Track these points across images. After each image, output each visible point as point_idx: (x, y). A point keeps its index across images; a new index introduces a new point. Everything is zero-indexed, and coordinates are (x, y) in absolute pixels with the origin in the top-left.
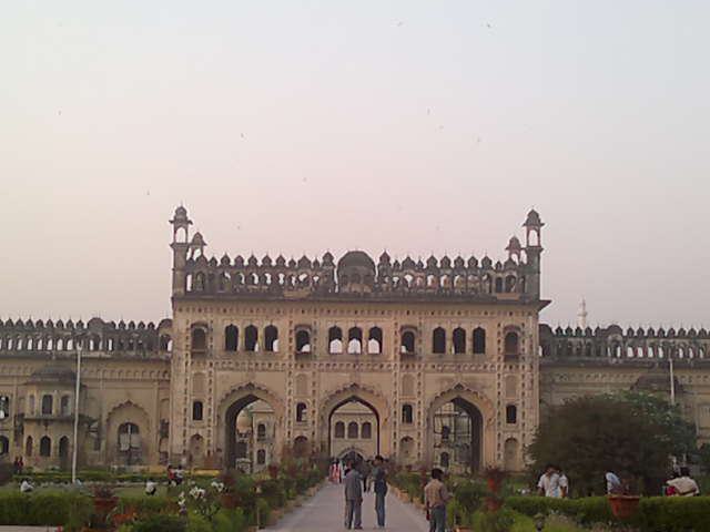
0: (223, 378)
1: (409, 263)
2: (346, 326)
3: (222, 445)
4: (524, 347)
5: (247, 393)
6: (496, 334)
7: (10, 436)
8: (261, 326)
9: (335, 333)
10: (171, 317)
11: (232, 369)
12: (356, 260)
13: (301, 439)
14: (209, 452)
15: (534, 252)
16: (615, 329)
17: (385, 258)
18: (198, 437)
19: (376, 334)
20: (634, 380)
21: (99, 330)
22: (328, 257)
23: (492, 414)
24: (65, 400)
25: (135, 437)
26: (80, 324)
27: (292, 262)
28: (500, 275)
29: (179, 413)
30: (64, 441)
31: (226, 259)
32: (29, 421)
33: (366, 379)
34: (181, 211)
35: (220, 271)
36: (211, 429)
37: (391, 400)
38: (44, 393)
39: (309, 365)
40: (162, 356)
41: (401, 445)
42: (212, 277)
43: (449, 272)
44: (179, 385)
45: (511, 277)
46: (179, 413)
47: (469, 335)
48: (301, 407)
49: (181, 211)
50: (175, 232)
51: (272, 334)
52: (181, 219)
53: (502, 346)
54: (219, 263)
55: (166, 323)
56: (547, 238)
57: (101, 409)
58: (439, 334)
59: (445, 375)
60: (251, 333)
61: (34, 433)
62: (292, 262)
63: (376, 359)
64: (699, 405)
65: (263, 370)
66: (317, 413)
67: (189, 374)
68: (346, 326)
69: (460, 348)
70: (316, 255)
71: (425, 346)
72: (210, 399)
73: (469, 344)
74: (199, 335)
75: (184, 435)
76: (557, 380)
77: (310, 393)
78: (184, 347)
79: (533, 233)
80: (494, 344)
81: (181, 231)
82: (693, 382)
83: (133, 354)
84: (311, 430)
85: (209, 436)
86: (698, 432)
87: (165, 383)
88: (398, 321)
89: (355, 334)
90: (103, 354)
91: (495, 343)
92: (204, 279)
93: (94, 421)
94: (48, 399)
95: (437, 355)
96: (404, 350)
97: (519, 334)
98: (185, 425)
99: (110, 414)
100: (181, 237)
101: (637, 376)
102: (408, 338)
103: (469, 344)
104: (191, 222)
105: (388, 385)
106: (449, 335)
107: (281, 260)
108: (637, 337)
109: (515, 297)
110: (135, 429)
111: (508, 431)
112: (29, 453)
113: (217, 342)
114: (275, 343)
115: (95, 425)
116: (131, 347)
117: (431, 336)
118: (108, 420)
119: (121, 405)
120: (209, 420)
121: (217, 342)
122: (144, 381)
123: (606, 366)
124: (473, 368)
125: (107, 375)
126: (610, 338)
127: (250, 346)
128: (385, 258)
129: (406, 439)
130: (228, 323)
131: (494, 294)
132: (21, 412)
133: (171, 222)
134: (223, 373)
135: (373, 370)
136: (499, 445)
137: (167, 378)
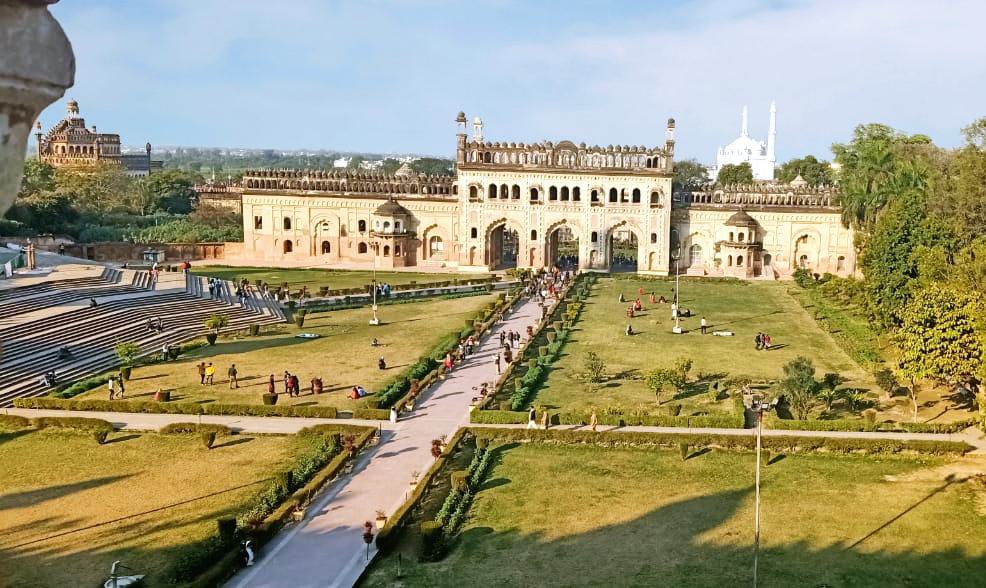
0: (489, 213)
2: (559, 181)
24: (397, 225)
33: (570, 216)
34: (463, 115)
41: (591, 255)
43: (620, 154)
44: (463, 219)
45: (656, 159)
52: (462, 118)
59: (615, 215)
60: (504, 187)
74: (473, 191)
83: (437, 196)
109: (657, 170)
110: (439, 240)
113: (483, 194)
116: (436, 193)
118: (424, 235)
119: (431, 227)
127: (505, 196)
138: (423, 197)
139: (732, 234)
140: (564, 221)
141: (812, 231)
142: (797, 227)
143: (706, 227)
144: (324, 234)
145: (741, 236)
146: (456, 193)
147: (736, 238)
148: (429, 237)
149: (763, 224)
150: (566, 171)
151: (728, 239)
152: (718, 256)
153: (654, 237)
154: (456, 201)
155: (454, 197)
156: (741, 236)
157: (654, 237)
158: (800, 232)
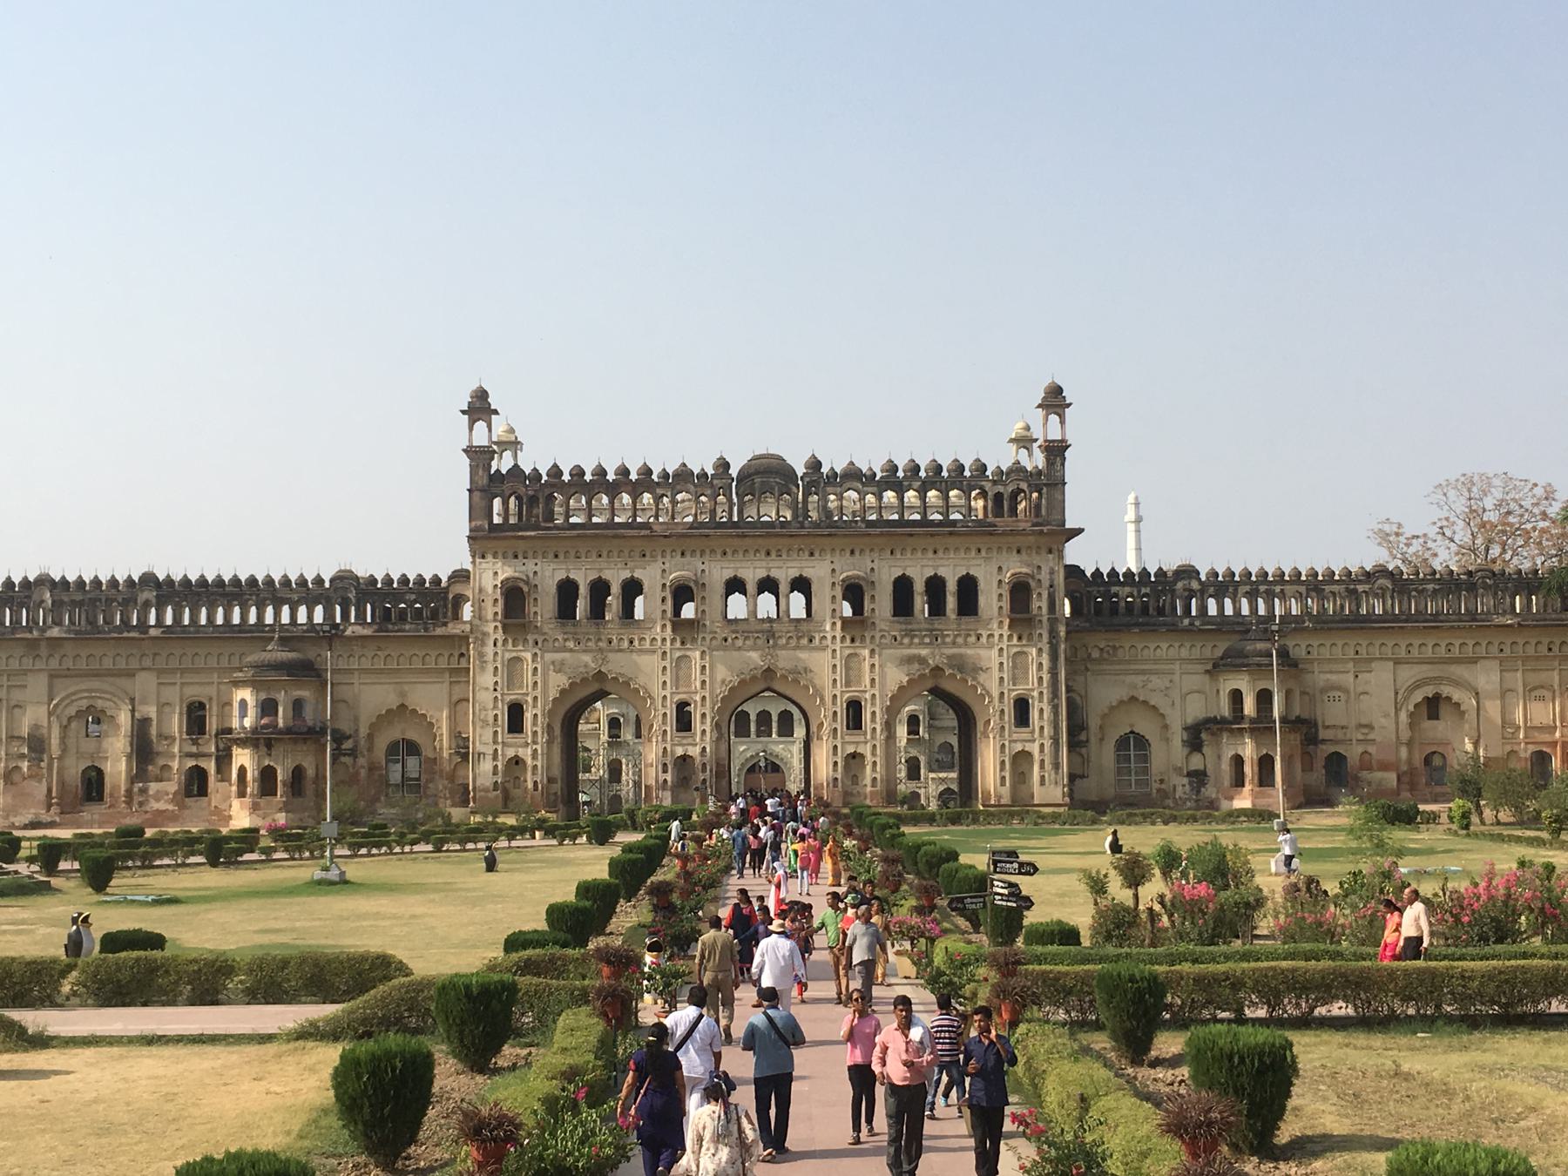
1: (853, 475)
2: (751, 573)
3: (557, 772)
4: (1039, 604)
5: (595, 687)
6: (995, 584)
7: (211, 766)
8: (616, 577)
9: (735, 585)
10: (470, 567)
11: (571, 650)
12: (767, 475)
13: (685, 758)
14: (535, 783)
15: (1056, 451)
16: (1188, 572)
17: (815, 465)
18: (517, 761)
19: (802, 585)
20: (1219, 653)
21: (347, 590)
22: (723, 465)
23: (993, 714)
24: (298, 705)
25: (412, 762)
26: (319, 581)
27: (665, 475)
28: (1000, 489)
29: (485, 723)
30: (298, 773)
31: (556, 471)
32: (242, 743)
33: (784, 660)
34: (481, 396)
35: (547, 492)
36: (539, 747)
37: (828, 699)
38: (263, 696)
39: (694, 640)
40: (453, 629)
41: (847, 767)
42: (533, 500)
44: (487, 679)
46: (485, 723)
47: (951, 586)
48: (682, 707)
49: (481, 396)
50: (471, 429)
51: (632, 589)
52: (479, 407)
53: (1006, 604)
54: (545, 478)
55: (461, 576)
56: (1077, 428)
57: (356, 719)
58: (903, 587)
60: (600, 589)
61: (242, 758)
62: (665, 475)
63: (804, 627)
64: (1323, 691)
65: (621, 651)
66: (708, 720)
67: (499, 658)
68: (751, 573)
69: (937, 608)
70: (702, 463)
71: (881, 604)
72: (535, 698)
73: (951, 602)
74: (514, 597)
75: (495, 758)
76: (1096, 654)
77: (698, 684)
78: (490, 616)
79: (1054, 418)
80: (992, 600)
81: (480, 426)
82: (1315, 655)
83: (407, 627)
84: (700, 744)
85: (534, 755)
86: (1322, 734)
87: (460, 674)
88: (837, 566)
89: (767, 585)
90: (360, 630)
91: (995, 597)
92: (516, 503)
93: (349, 737)
94: (268, 707)
95: (902, 619)
96: (847, 610)
97: (1033, 584)
98: (495, 742)
99: (372, 726)
100: (481, 437)
101: (1222, 646)
102: (854, 592)
103: (951, 602)
104: (495, 412)
105: (825, 668)
106: (919, 587)
107: (646, 471)
108: (1223, 585)
110: (412, 748)
111: (1020, 740)
112: (241, 794)
113: (544, 607)
114: (639, 601)
115: (348, 745)
116: (402, 616)
117: (890, 588)
118: (370, 737)
120: (535, 733)
121: (544, 607)
122: (428, 671)
123: (1174, 629)
124: (960, 640)
125: (366, 663)
126: (1180, 585)
127: (597, 610)
128: (815, 465)
129: (854, 756)
130: (561, 575)
131: (991, 519)
132: (227, 725)
133: (463, 412)
134: (558, 656)
135: (797, 647)
136: (1003, 762)
137: (463, 664)
138: (367, 632)
139: (1237, 697)
140: (769, 672)
141: (1457, 683)
142: (1409, 674)
143: (1157, 682)
144: (88, 746)
145: (1264, 698)
146: (457, 616)
147: (1249, 707)
148: (382, 744)
149: (1320, 677)
150: (771, 536)
151: (1225, 710)
152: (1196, 762)
153: (1022, 709)
154: (464, 639)
155: (453, 629)
156: (1264, 698)
157: (1022, 709)
158: (1417, 685)
